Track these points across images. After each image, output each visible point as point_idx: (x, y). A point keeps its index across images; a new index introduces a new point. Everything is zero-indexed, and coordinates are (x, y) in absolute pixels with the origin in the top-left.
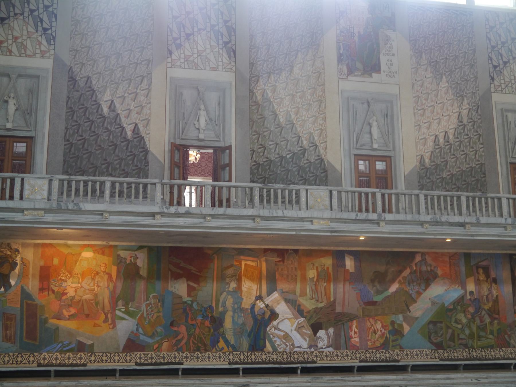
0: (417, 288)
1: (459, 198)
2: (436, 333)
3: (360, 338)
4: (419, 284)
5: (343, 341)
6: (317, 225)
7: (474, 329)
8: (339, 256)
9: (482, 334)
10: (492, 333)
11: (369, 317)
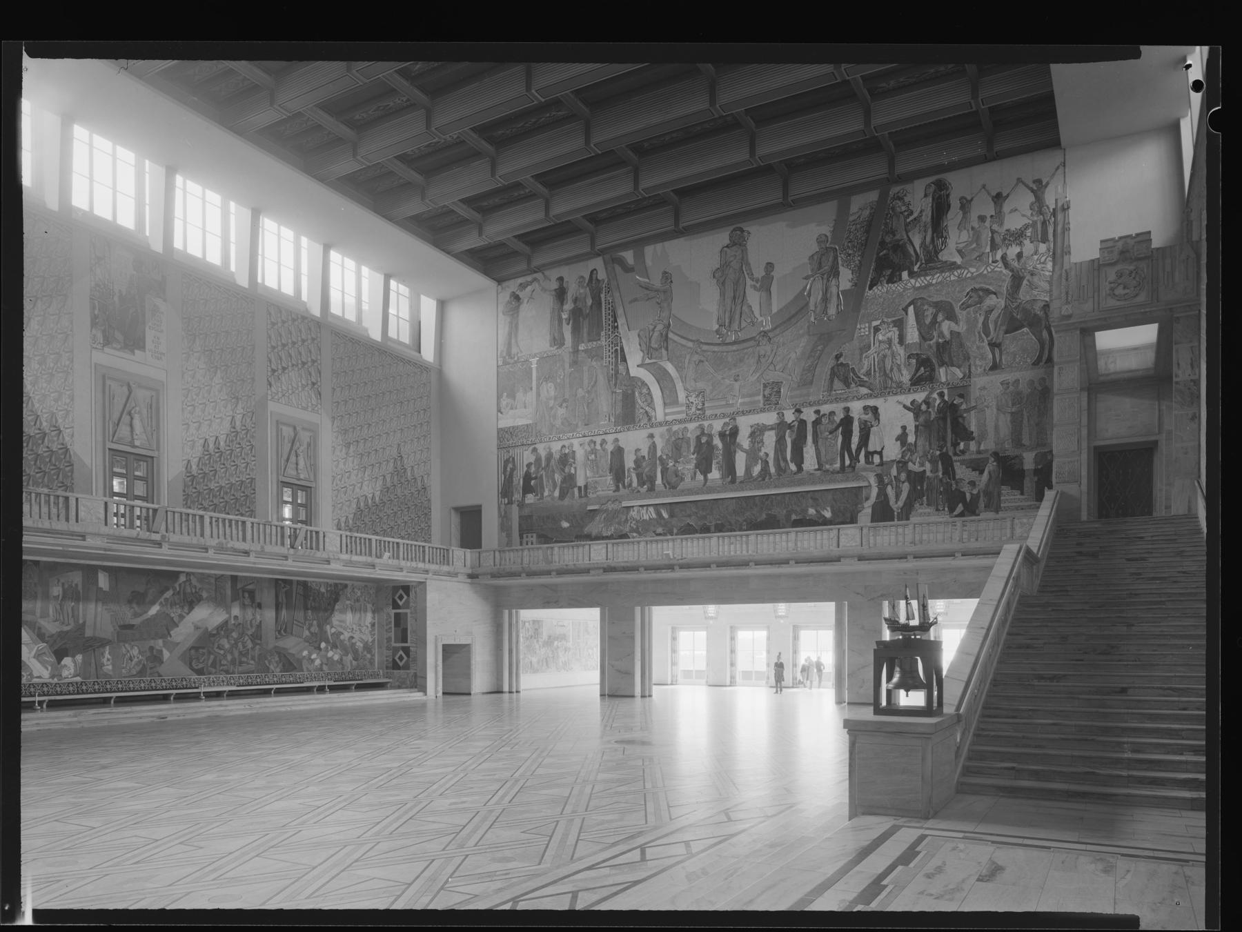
0: (179, 611)
1: (244, 523)
2: (198, 659)
3: (114, 666)
4: (182, 607)
5: (93, 670)
6: (90, 541)
7: (236, 654)
8: (90, 572)
9: (244, 659)
10: (253, 659)
11: (125, 642)
